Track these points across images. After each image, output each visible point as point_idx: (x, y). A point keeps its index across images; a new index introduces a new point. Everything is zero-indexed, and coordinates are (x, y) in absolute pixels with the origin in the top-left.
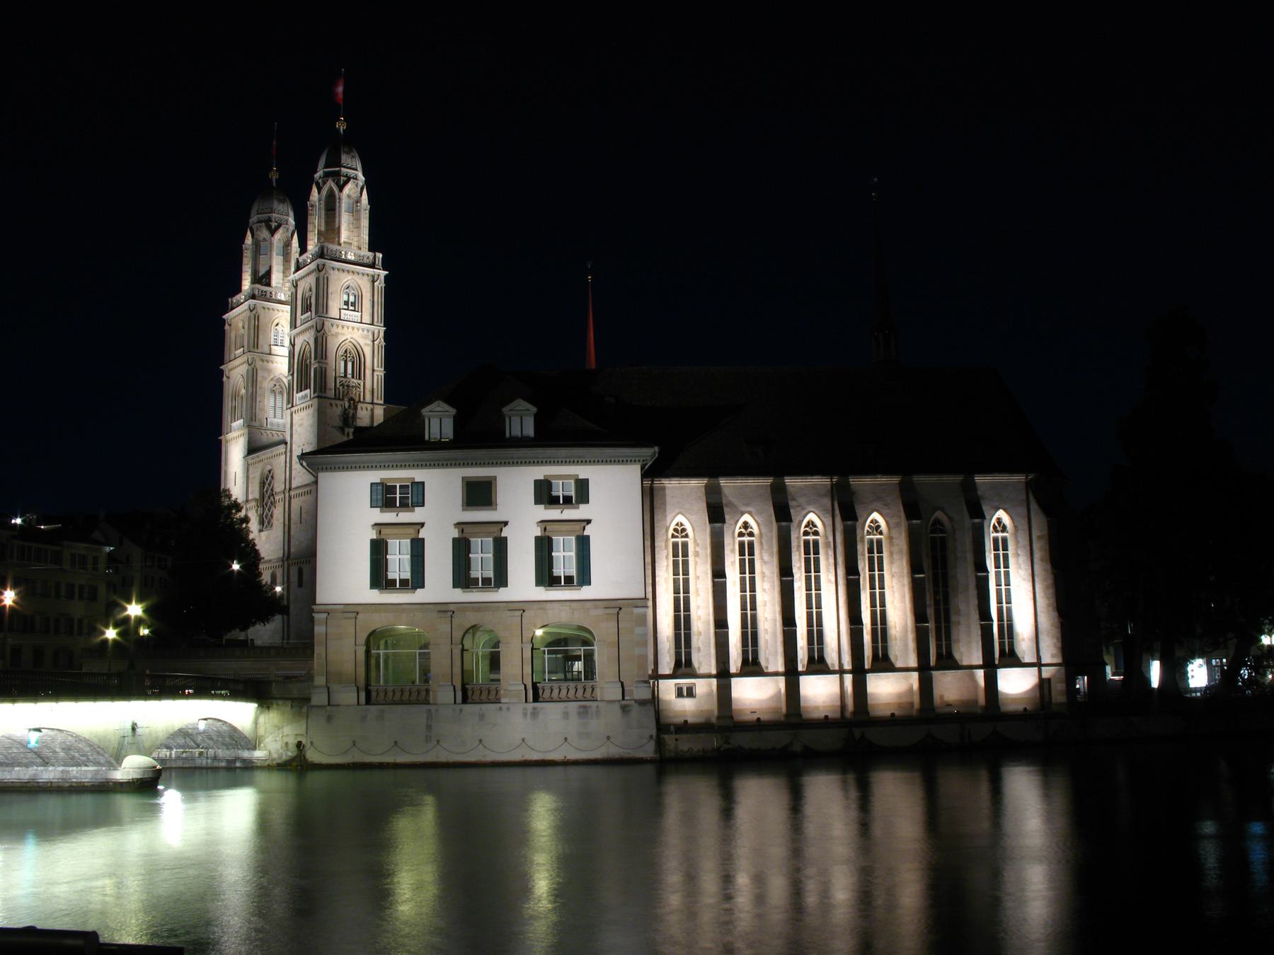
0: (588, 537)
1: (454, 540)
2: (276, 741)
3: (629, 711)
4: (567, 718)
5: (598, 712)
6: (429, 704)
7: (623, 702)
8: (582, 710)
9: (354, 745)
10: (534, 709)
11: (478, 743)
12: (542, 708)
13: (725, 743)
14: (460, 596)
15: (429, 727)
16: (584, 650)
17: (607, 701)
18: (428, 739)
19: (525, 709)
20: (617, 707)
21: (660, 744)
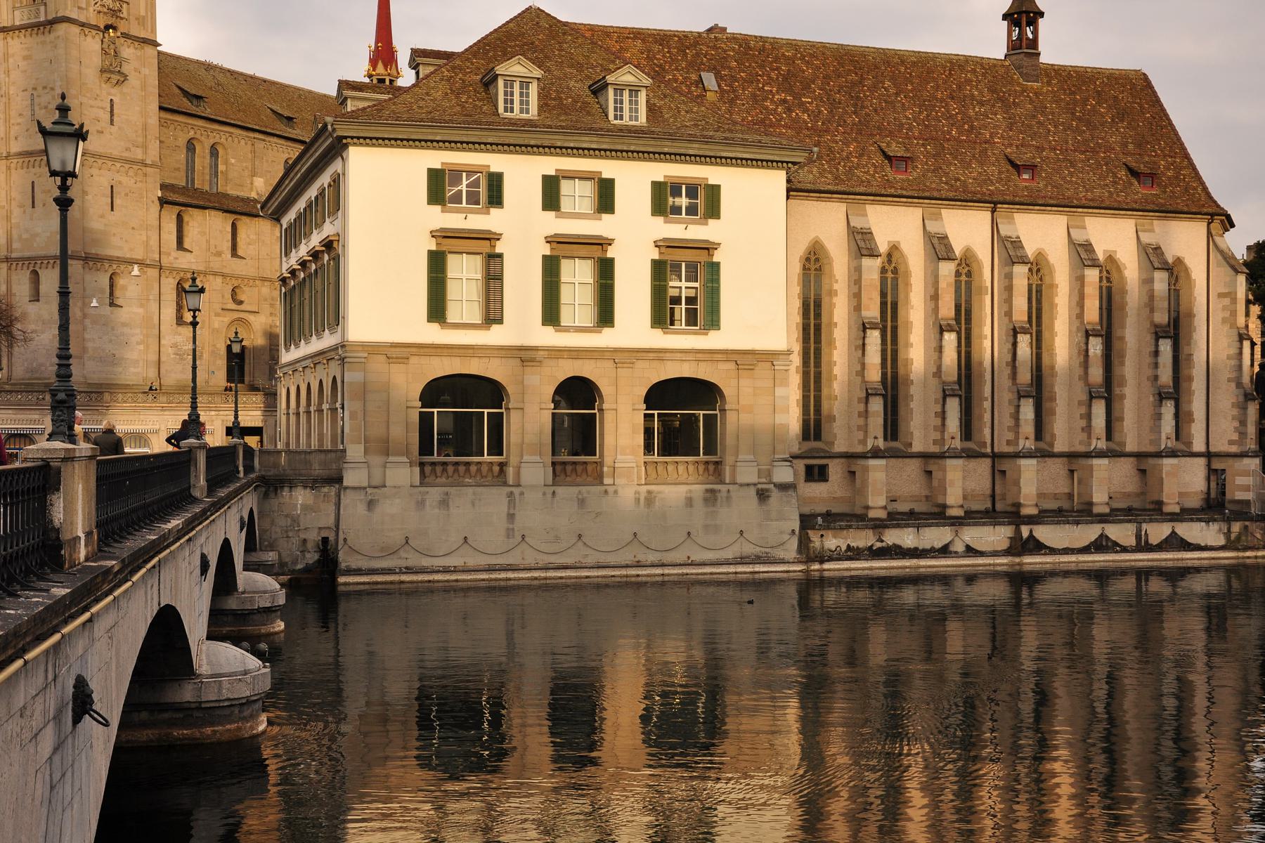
0: (718, 264)
1: (544, 257)
2: (288, 537)
3: (768, 497)
5: (728, 498)
6: (505, 484)
7: (760, 486)
8: (708, 495)
11: (575, 539)
12: (659, 492)
14: (547, 337)
15: (511, 517)
16: (704, 414)
17: (741, 485)
18: (510, 533)
20: (753, 491)
21: (804, 543)
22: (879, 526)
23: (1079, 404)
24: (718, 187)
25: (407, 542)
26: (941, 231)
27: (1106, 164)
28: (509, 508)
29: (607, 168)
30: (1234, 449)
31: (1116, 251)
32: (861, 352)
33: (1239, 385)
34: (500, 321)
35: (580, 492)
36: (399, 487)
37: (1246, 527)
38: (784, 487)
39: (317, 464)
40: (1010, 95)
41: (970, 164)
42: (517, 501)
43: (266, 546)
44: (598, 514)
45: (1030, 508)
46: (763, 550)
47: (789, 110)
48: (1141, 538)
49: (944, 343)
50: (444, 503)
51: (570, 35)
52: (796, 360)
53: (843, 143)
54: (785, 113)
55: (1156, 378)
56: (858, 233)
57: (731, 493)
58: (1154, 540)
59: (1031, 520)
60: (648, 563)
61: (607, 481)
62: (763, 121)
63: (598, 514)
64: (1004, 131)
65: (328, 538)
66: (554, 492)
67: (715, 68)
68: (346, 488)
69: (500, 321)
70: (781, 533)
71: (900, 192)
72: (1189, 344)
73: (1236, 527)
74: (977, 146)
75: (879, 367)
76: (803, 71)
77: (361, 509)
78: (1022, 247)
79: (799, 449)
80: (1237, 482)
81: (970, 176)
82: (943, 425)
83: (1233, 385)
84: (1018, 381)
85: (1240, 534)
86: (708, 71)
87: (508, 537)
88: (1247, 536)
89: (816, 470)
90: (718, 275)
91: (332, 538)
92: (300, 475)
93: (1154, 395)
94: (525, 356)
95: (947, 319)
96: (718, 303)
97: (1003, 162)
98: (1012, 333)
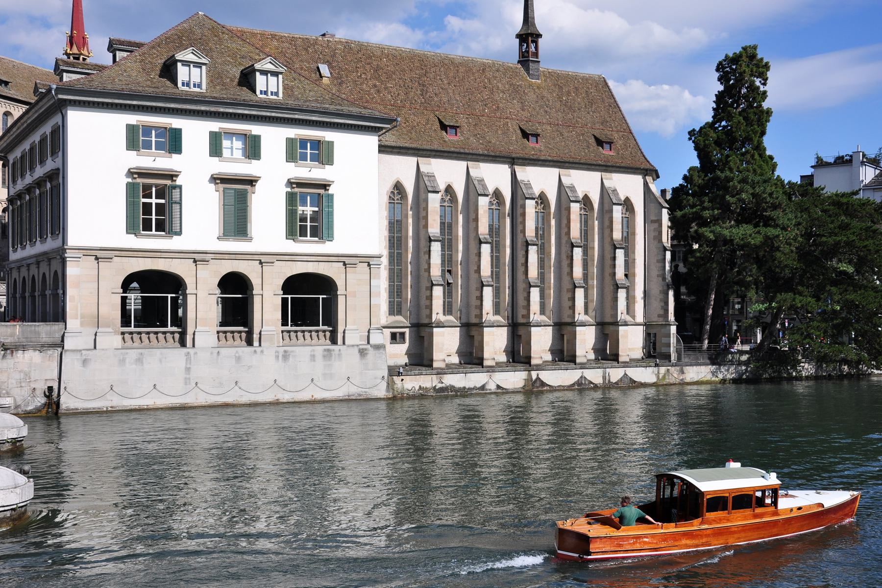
0: (332, 195)
2: (21, 387)
3: (366, 354)
4: (314, 361)
5: (340, 355)
7: (361, 347)
8: (326, 353)
9: (111, 389)
10: (285, 351)
12: (292, 352)
13: (439, 383)
15: (188, 370)
17: (349, 346)
18: (187, 381)
19: (277, 352)
20: (356, 350)
21: (390, 385)
22: (440, 372)
23: (567, 291)
24: (333, 142)
25: (111, 389)
26: (479, 176)
27: (583, 134)
28: (186, 364)
29: (255, 129)
30: (661, 321)
31: (589, 192)
32: (427, 256)
33: (664, 279)
34: (179, 233)
35: (237, 352)
36: (106, 350)
37: (668, 370)
38: (378, 347)
39: (44, 334)
40: (521, 87)
41: (497, 132)
42: (192, 359)
43: (4, 394)
44: (250, 367)
45: (537, 360)
46: (362, 389)
47: (378, 91)
48: (606, 378)
49: (482, 250)
50: (139, 360)
51: (227, 34)
52: (385, 261)
53: (415, 115)
54: (375, 93)
55: (614, 274)
56: (426, 176)
57: (341, 352)
58: (614, 379)
59: (539, 368)
60: (285, 401)
61: (256, 343)
62: (361, 98)
63: (250, 367)
64: (518, 111)
65: (52, 387)
66: (218, 352)
67: (328, 61)
68: (66, 351)
69: (179, 233)
70: (376, 378)
71: (452, 149)
72: (634, 252)
73: (663, 370)
74: (502, 120)
75: (440, 266)
76: (388, 66)
77: (78, 365)
78: (531, 188)
79: (387, 321)
80: (663, 342)
81: (497, 142)
82: (482, 305)
83: (660, 279)
84: (529, 276)
85: (665, 374)
86: (323, 63)
87: (186, 384)
88: (669, 376)
89: (398, 335)
90: (332, 203)
91: (56, 387)
92: (31, 342)
93: (613, 285)
94: (198, 258)
95: (484, 235)
96: (332, 221)
97: (519, 132)
98: (525, 244)
